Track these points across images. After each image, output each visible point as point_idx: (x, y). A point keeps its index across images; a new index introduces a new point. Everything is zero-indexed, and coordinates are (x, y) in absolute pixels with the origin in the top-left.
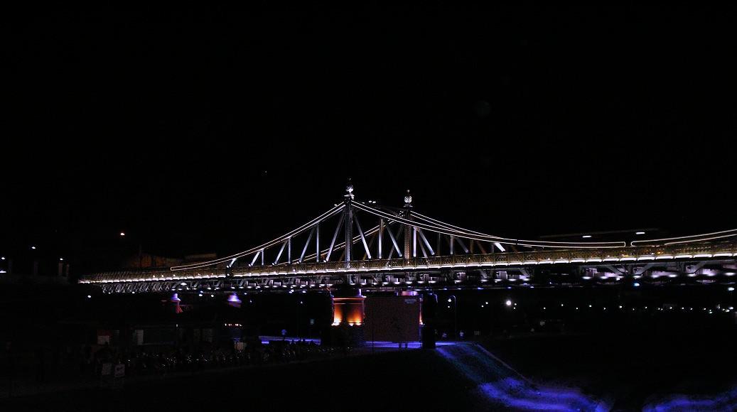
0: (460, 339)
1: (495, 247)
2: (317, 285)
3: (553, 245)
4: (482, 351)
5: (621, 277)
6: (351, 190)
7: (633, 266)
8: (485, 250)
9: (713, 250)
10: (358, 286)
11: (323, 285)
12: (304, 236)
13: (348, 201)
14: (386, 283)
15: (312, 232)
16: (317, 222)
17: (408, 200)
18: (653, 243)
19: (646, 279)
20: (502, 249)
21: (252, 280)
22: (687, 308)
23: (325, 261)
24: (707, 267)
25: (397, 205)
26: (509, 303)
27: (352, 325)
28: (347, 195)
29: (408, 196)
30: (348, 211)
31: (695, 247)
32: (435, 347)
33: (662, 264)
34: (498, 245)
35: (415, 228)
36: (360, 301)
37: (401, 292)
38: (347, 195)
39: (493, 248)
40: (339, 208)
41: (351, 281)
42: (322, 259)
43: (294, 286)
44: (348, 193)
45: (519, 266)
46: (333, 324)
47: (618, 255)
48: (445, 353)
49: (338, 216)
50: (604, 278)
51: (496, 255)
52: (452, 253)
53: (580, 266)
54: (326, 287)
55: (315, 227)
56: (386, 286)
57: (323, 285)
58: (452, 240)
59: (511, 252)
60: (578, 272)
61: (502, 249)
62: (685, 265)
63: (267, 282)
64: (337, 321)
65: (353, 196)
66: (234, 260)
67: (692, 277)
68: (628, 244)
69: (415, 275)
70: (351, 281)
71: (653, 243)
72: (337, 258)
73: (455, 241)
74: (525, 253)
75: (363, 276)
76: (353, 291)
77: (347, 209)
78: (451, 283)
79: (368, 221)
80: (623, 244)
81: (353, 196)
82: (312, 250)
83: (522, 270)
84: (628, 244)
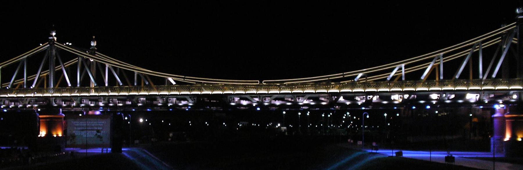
0: (136, 146)
1: (169, 81)
2: (25, 106)
3: (236, 82)
4: (148, 154)
5: (256, 104)
6: (54, 34)
7: (263, 97)
8: (161, 83)
9: (316, 88)
10: (60, 106)
11: (29, 106)
12: (13, 68)
13: (52, 42)
14: (83, 105)
15: (20, 64)
16: (24, 57)
17: (93, 44)
18: (277, 82)
19: (260, 104)
20: (174, 83)
21: (12, 100)
22: (190, 123)
23: (32, 87)
24: (276, 99)
25: (86, 47)
26: (141, 120)
27: (55, 136)
28: (51, 38)
29: (94, 41)
30: (51, 50)
31: (303, 86)
32: (122, 151)
33: (282, 96)
34: (171, 80)
35: (107, 65)
36: (61, 118)
37: (87, 112)
38: (51, 38)
39: (166, 81)
40: (43, 47)
41: (54, 103)
42: (30, 83)
43: (4, 106)
44: (52, 36)
45: (187, 95)
46: (39, 136)
47: (303, 88)
48: (128, 156)
49: (43, 52)
50: (180, 104)
51: (170, 87)
52: (135, 84)
53: (229, 96)
54: (32, 107)
55: (23, 61)
56: (83, 107)
57: (29, 106)
58: (136, 75)
59: (180, 85)
60: (227, 99)
61: (174, 83)
62: (263, 97)
63: (3, 101)
64: (43, 133)
65: (55, 38)
66: (360, 75)
67: (233, 105)
68: (261, 82)
69: (106, 99)
70: (54, 103)
71: (277, 82)
72: (42, 86)
73: (138, 76)
74: (190, 87)
75: (64, 99)
76: (56, 110)
77: (51, 48)
78: (134, 105)
79: (66, 56)
80: (257, 82)
81: (55, 38)
82: (20, 76)
83: (187, 97)
84: (261, 82)
